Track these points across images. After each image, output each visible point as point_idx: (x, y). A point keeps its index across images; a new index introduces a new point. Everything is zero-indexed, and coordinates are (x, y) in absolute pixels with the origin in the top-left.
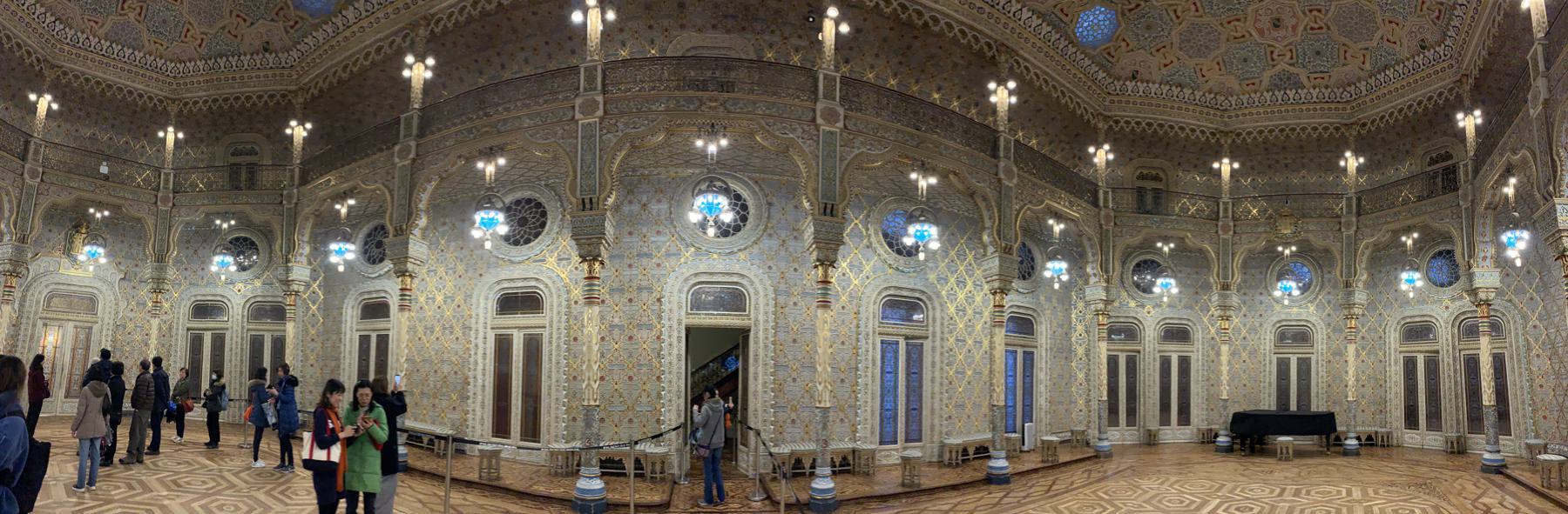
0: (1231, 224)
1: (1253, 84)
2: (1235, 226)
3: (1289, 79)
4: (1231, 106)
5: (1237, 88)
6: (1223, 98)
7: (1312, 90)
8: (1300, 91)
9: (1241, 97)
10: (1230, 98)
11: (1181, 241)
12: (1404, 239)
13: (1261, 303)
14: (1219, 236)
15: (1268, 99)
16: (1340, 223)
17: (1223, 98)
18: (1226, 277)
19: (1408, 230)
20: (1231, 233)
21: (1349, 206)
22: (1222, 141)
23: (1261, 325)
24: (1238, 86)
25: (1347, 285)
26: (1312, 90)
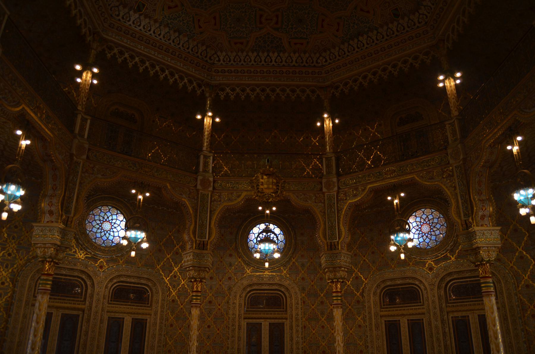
0: (211, 179)
1: (242, 43)
2: (214, 182)
4: (219, 61)
7: (292, 55)
8: (281, 54)
10: (219, 53)
11: (157, 191)
12: (389, 198)
13: (231, 265)
14: (198, 190)
15: (253, 58)
16: (321, 183)
18: (202, 235)
19: (394, 190)
20: (211, 189)
21: (329, 166)
22: (207, 95)
23: (230, 289)
25: (332, 247)
26: (292, 55)
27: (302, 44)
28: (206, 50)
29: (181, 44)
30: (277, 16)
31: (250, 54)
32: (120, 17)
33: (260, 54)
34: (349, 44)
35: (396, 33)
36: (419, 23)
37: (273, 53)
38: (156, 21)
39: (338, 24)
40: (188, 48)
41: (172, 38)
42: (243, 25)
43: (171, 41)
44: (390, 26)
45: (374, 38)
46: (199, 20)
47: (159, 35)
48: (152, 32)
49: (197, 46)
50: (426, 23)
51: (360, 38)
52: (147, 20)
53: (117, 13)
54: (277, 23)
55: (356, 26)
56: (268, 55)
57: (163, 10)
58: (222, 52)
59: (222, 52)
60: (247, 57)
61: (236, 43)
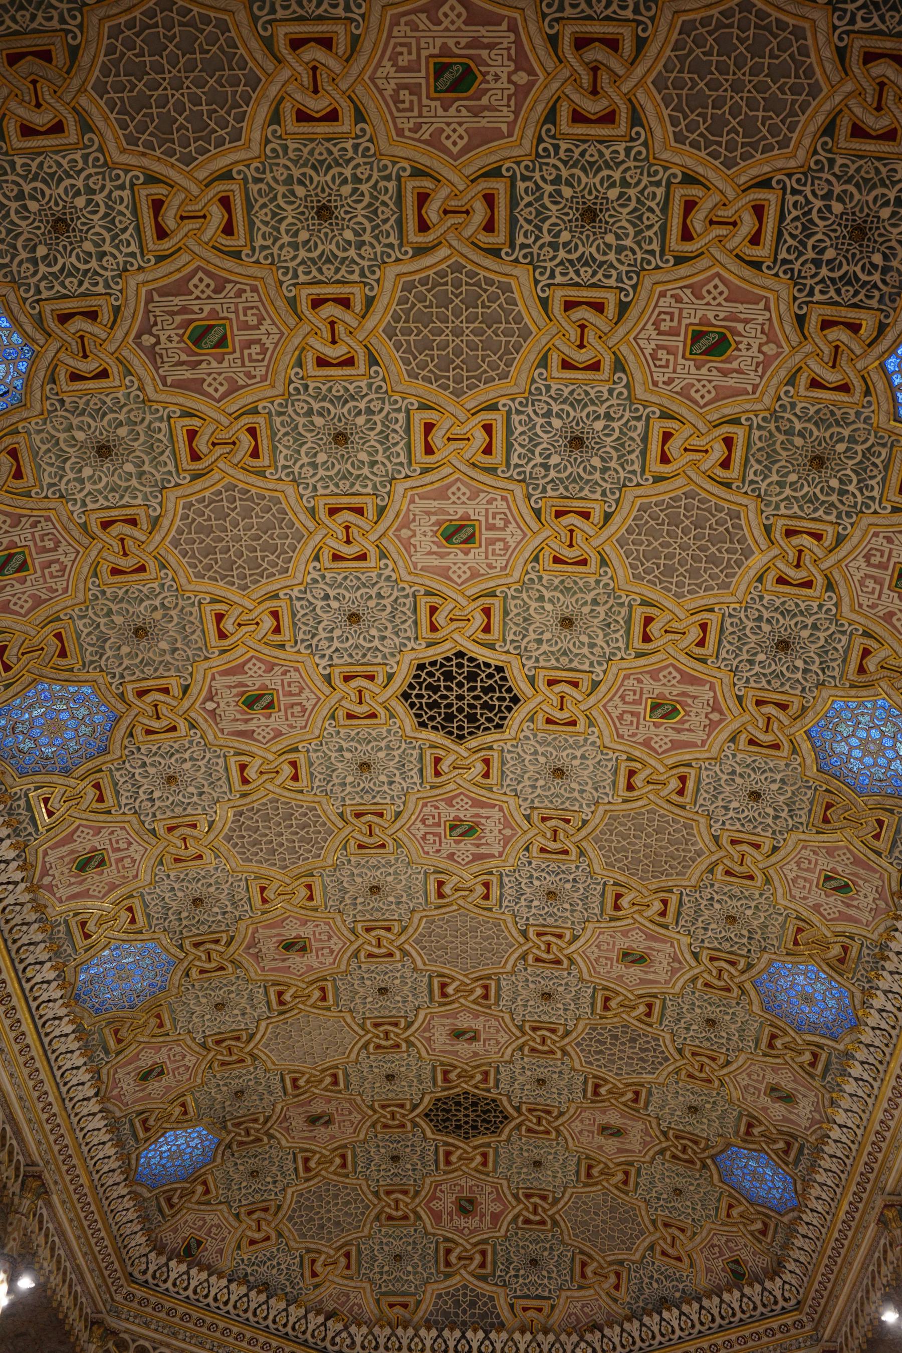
1: (405, 1306)
3: (473, 1304)
5: (370, 1309)
6: (339, 1326)
7: (517, 1336)
9: (376, 1330)
10: (353, 1329)
17: (339, 1326)
24: (373, 1306)
26: (517, 1336)
27: (540, 1310)
28: (324, 1324)
29: (271, 1317)
30: (483, 1253)
31: (423, 1332)
32: (149, 1276)
33: (446, 1333)
34: (642, 1325)
35: (739, 1315)
36: (785, 1300)
37: (475, 1331)
38: (220, 1276)
39: (618, 1275)
40: (285, 1325)
41: (253, 1305)
42: (410, 1269)
43: (250, 1315)
44: (726, 1296)
45: (695, 1317)
46: (313, 1262)
47: (226, 1303)
48: (210, 1300)
49: (305, 1317)
50: (799, 1303)
51: (666, 1314)
52: (204, 1275)
53: (144, 1266)
54: (483, 1265)
55: (655, 1285)
56: (463, 1336)
57: (239, 1247)
58: (359, 1325)
59: (359, 1325)
60: (416, 1340)
61: (391, 1306)
